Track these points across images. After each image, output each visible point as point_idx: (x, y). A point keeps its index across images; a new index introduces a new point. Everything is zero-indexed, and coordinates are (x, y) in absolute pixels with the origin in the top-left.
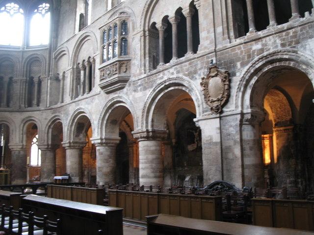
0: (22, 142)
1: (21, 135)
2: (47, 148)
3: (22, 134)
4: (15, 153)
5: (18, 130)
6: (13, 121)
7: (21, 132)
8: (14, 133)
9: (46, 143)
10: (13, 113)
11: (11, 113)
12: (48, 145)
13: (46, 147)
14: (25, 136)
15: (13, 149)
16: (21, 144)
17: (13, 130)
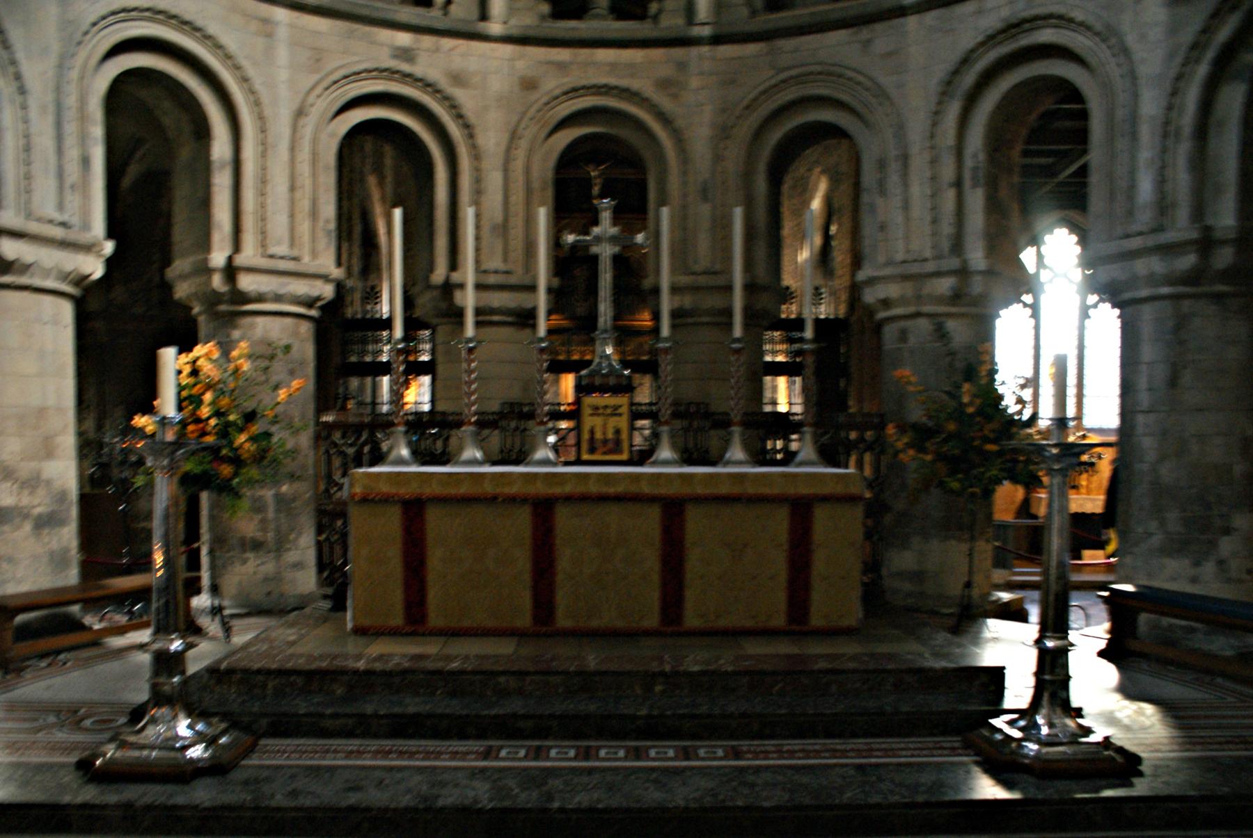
0: (958, 246)
1: (951, 194)
2: (1192, 278)
3: (958, 184)
4: (903, 336)
5: (919, 161)
6: (881, 93)
7: (948, 172)
8: (894, 178)
9: (1181, 228)
10: (879, 27)
11: (865, 33)
12: (1206, 243)
13: (1187, 261)
14: (976, 200)
15: (886, 303)
16: (954, 263)
17: (882, 164)
